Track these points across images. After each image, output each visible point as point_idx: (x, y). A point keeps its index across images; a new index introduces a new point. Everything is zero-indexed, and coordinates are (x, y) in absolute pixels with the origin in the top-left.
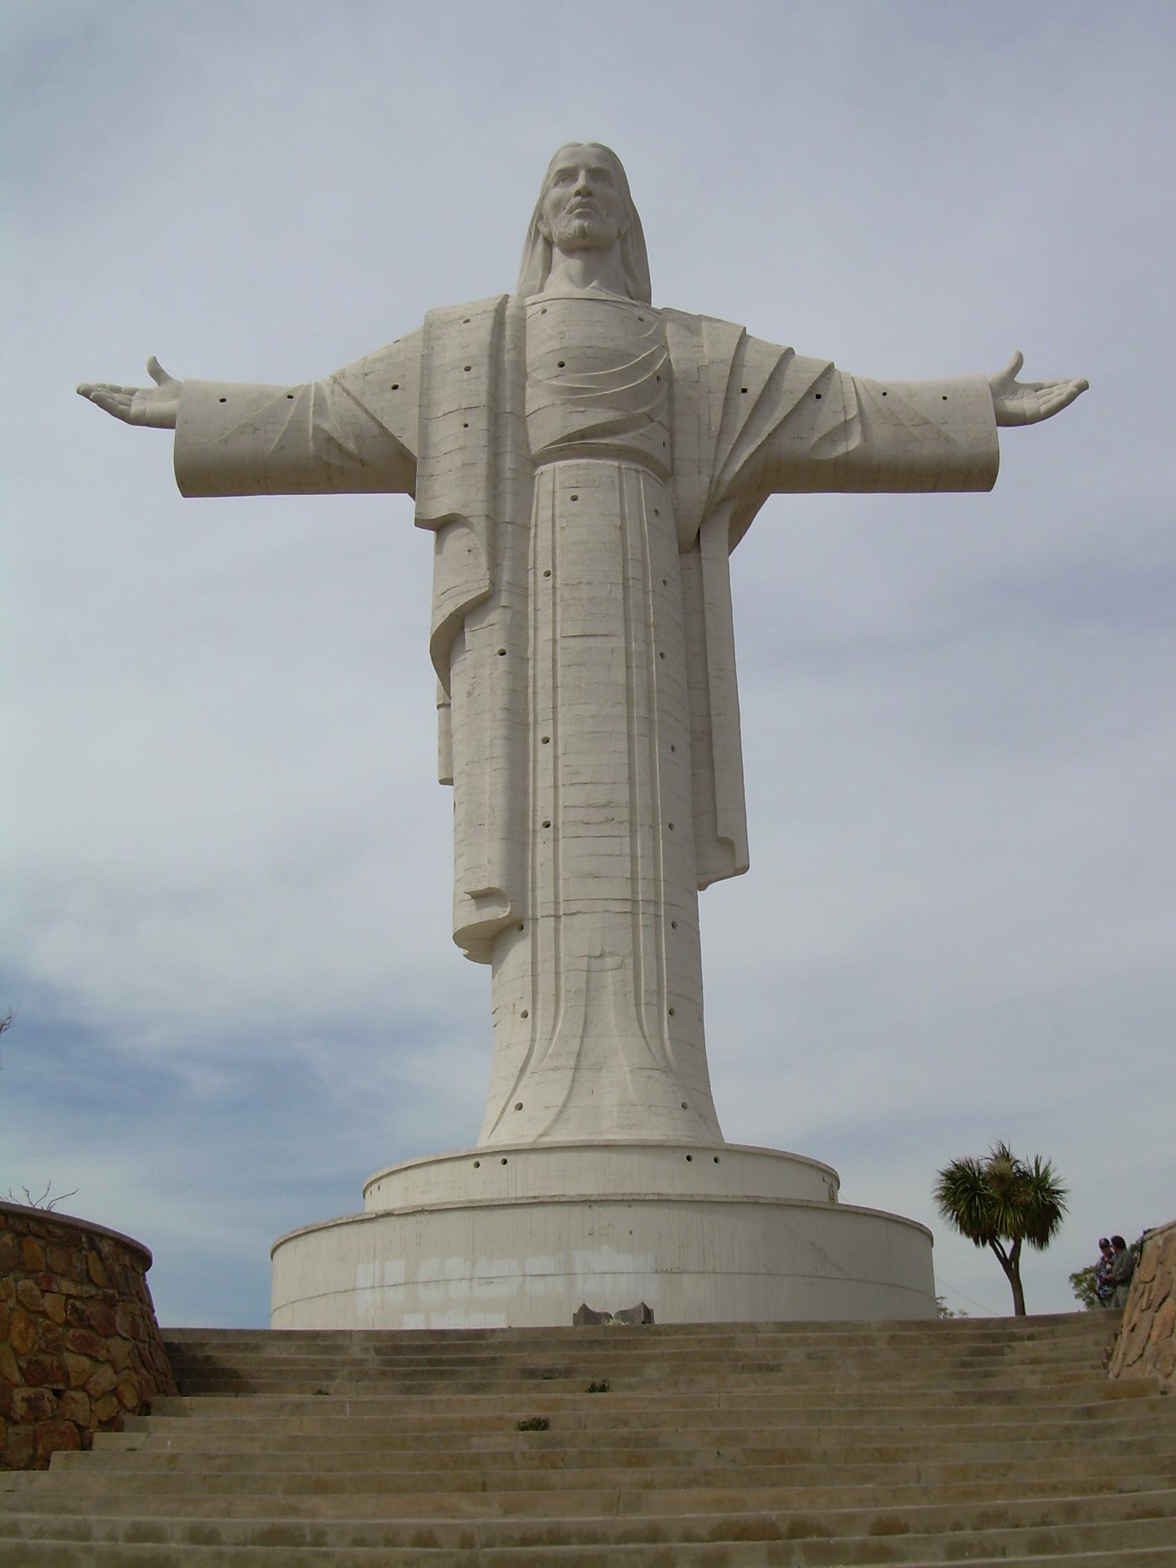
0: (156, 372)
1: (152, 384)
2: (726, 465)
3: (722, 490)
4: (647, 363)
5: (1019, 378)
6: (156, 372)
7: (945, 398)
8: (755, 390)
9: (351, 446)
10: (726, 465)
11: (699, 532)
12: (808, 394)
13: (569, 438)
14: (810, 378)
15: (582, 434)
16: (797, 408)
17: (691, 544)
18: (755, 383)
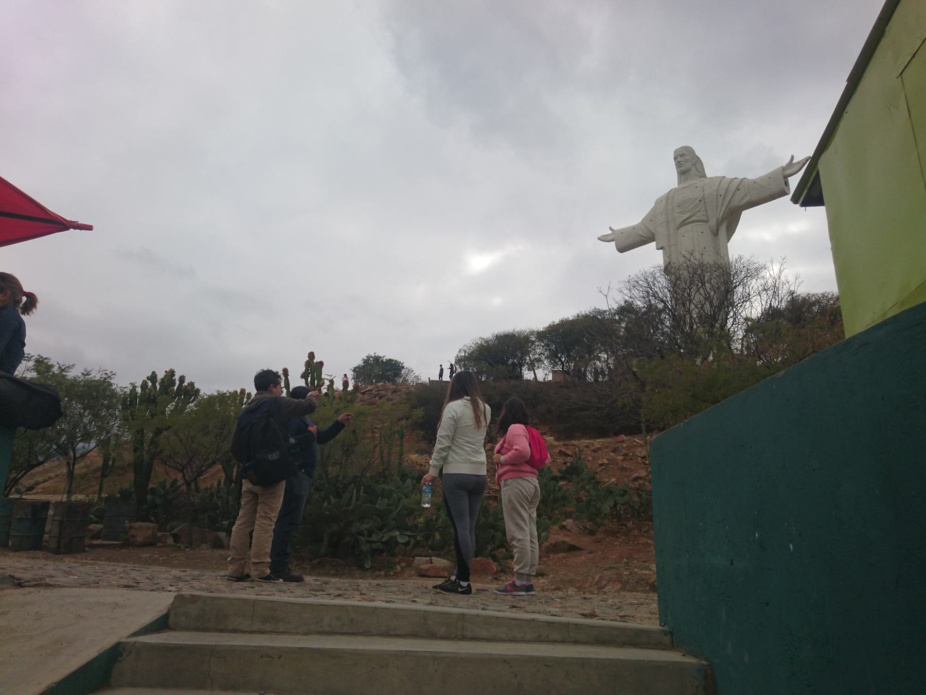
0: (611, 229)
1: (611, 232)
2: (719, 214)
3: (720, 220)
4: (697, 198)
5: (794, 162)
6: (611, 229)
7: (770, 178)
8: (723, 196)
9: (645, 236)
10: (719, 214)
11: (718, 230)
12: (735, 191)
13: (682, 223)
14: (736, 186)
15: (684, 221)
16: (734, 195)
17: (716, 234)
18: (722, 193)
